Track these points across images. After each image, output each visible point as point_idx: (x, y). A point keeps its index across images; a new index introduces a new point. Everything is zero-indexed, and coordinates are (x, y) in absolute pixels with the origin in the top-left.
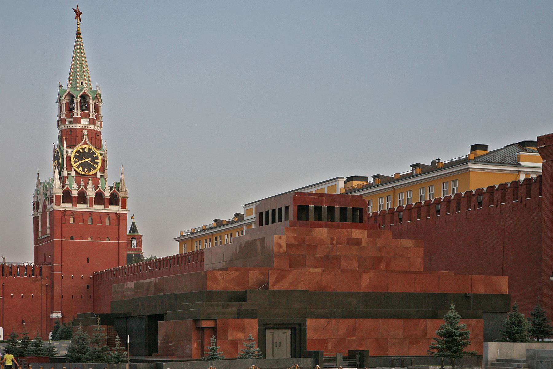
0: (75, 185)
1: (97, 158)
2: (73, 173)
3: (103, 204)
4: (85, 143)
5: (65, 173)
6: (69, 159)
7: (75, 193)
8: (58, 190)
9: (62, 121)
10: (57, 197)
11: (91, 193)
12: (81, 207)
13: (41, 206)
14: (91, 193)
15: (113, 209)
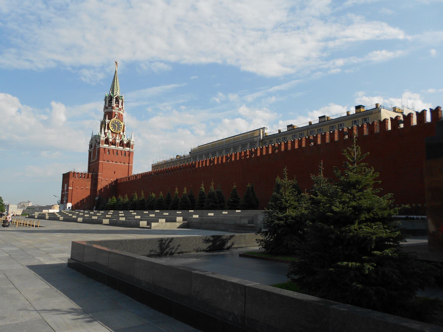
0: (110, 137)
1: (121, 125)
2: (110, 131)
3: (123, 146)
4: (116, 118)
5: (106, 131)
6: (108, 125)
7: (111, 140)
8: (103, 137)
9: (106, 108)
10: (102, 141)
11: (118, 141)
12: (113, 147)
13: (93, 146)
14: (118, 141)
15: (128, 149)
